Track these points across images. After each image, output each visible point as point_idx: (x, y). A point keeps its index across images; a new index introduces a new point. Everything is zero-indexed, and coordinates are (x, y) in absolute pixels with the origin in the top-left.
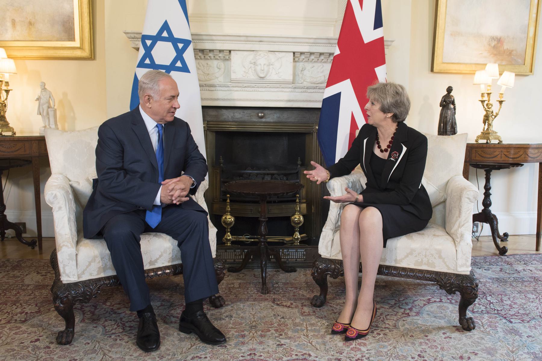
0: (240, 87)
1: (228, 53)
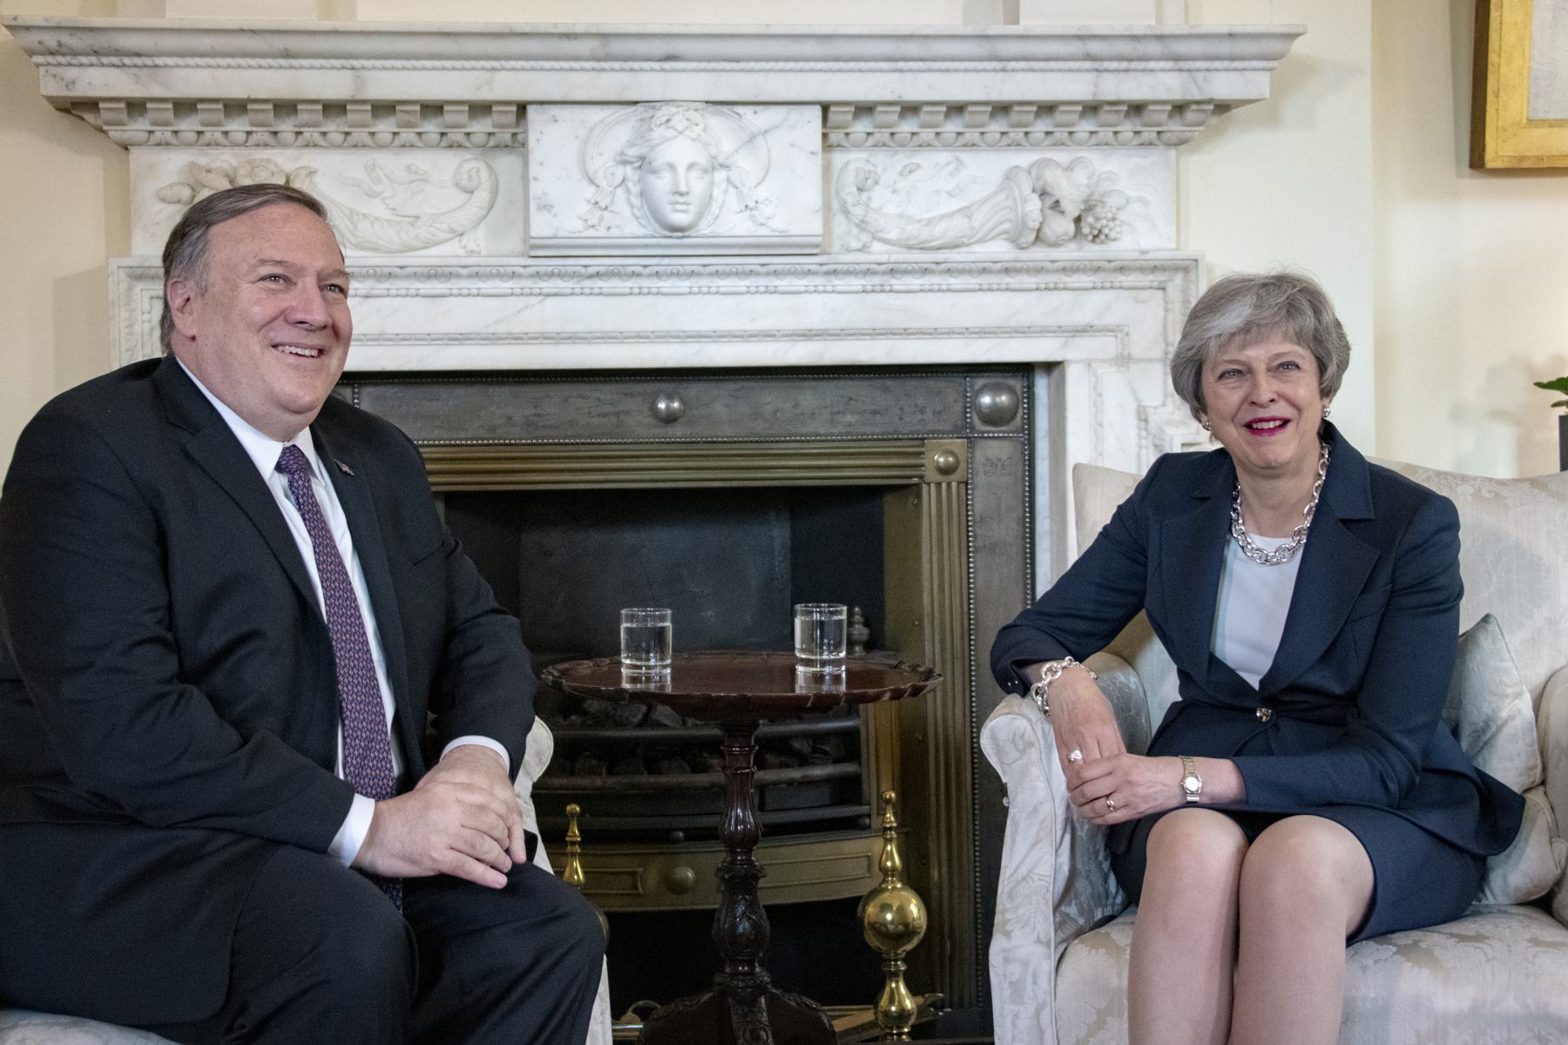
0: (573, 275)
1: (512, 118)
